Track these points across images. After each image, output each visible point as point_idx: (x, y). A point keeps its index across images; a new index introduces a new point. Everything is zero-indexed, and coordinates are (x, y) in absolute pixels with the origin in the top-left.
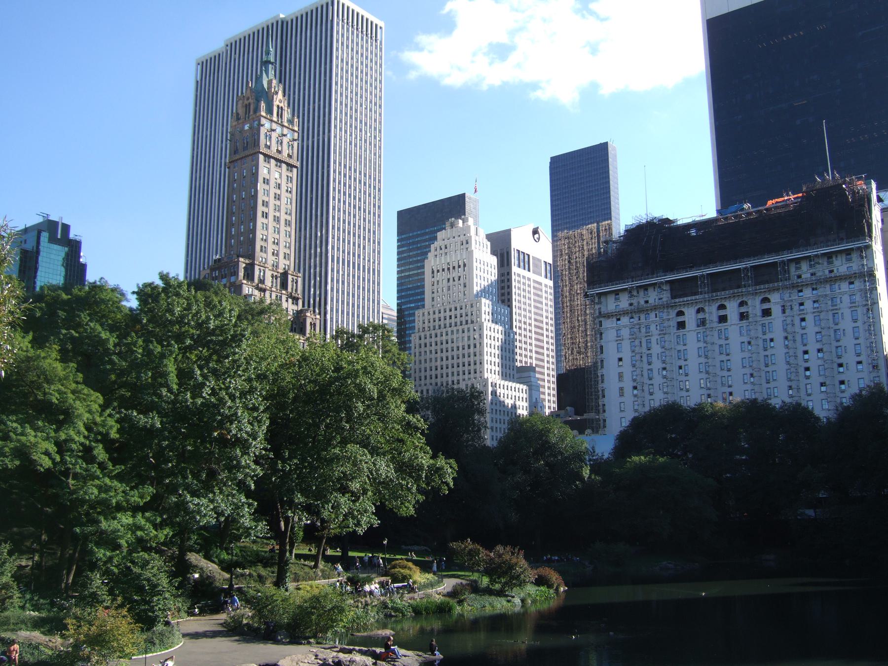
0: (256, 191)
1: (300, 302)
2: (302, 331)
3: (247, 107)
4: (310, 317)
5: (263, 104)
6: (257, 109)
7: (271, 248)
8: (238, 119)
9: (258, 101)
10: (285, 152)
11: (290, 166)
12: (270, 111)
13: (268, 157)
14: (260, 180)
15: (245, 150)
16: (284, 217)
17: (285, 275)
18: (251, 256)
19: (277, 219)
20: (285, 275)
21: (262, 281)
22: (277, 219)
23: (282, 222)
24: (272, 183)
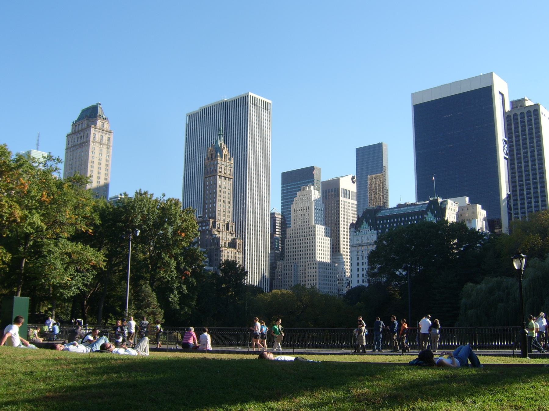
0: (216, 191)
1: (234, 235)
2: (235, 247)
3: (212, 155)
4: (238, 241)
5: (218, 154)
6: (216, 157)
7: (222, 213)
8: (208, 159)
9: (216, 153)
10: (228, 173)
11: (230, 179)
12: (221, 157)
13: (220, 176)
14: (218, 186)
15: (211, 172)
16: (227, 200)
17: (228, 224)
18: (214, 218)
19: (224, 202)
20: (228, 224)
21: (219, 228)
22: (224, 202)
23: (227, 202)
24: (223, 187)
